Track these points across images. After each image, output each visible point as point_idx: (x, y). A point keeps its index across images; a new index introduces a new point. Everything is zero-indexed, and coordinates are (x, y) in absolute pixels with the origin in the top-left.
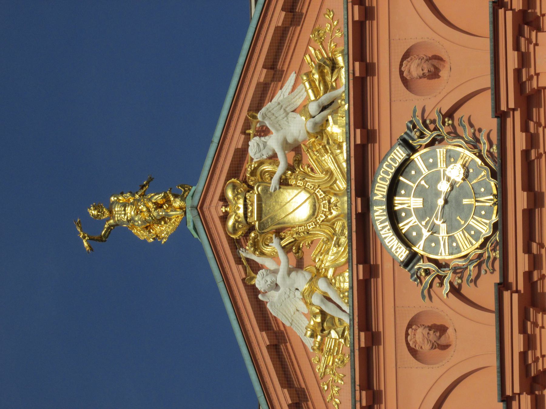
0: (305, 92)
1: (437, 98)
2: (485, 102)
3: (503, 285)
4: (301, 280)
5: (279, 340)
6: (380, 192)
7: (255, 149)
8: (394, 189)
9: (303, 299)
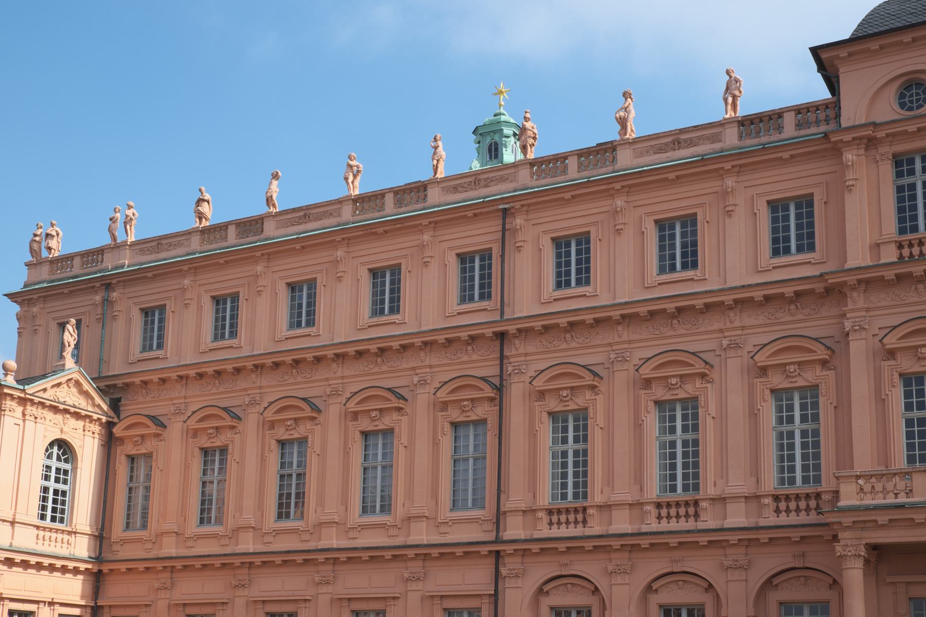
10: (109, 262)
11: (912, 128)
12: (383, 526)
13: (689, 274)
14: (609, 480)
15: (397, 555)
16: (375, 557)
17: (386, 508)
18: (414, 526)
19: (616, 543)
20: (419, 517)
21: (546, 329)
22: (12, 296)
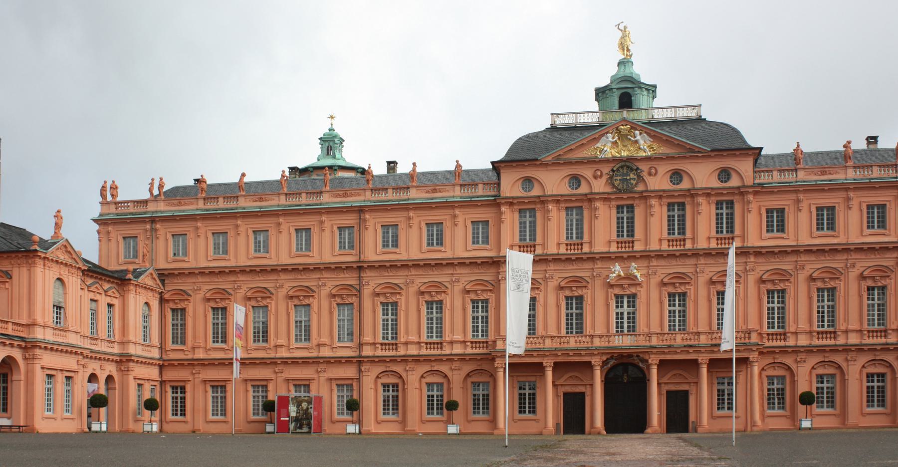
0: (649, 143)
3: (608, 193)
4: (609, 145)
6: (628, 164)
7: (637, 132)
10: (151, 207)
11: (526, 201)
12: (307, 348)
14: (407, 333)
15: (316, 361)
16: (305, 362)
17: (308, 339)
18: (322, 348)
19: (410, 359)
20: (325, 345)
21: (381, 267)
22: (95, 220)
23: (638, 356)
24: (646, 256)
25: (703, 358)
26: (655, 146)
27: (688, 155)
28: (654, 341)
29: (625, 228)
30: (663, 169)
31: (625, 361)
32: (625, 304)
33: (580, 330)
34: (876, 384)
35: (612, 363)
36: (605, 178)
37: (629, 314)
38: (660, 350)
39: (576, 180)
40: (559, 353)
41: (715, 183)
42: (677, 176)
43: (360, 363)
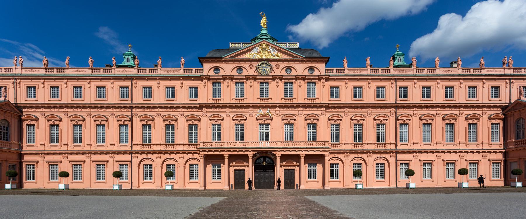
0: (276, 53)
1: (275, 68)
2: (274, 74)
3: (256, 76)
4: (256, 52)
5: (250, 50)
6: (266, 62)
8: (266, 64)
9: (255, 54)
13: (173, 99)
23: (271, 152)
24: (274, 106)
25: (303, 154)
26: (279, 54)
27: (295, 59)
28: (279, 145)
29: (264, 93)
30: (282, 65)
31: (264, 155)
32: (264, 128)
33: (242, 139)
34: (380, 168)
35: (258, 155)
36: (254, 69)
37: (266, 133)
38: (282, 149)
39: (240, 68)
40: (232, 150)
41: (307, 73)
42: (289, 68)
43: (132, 154)
